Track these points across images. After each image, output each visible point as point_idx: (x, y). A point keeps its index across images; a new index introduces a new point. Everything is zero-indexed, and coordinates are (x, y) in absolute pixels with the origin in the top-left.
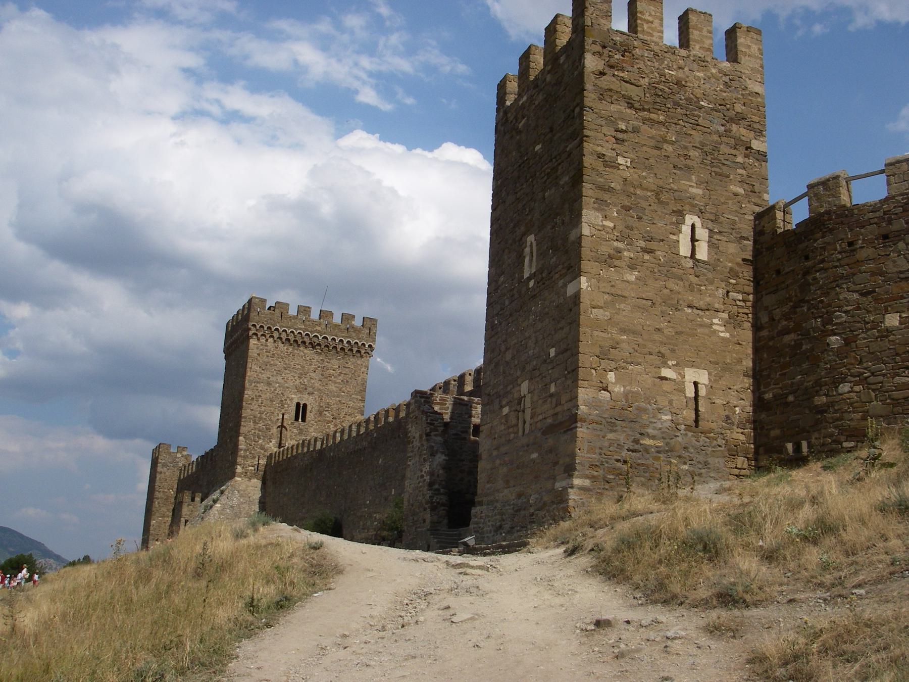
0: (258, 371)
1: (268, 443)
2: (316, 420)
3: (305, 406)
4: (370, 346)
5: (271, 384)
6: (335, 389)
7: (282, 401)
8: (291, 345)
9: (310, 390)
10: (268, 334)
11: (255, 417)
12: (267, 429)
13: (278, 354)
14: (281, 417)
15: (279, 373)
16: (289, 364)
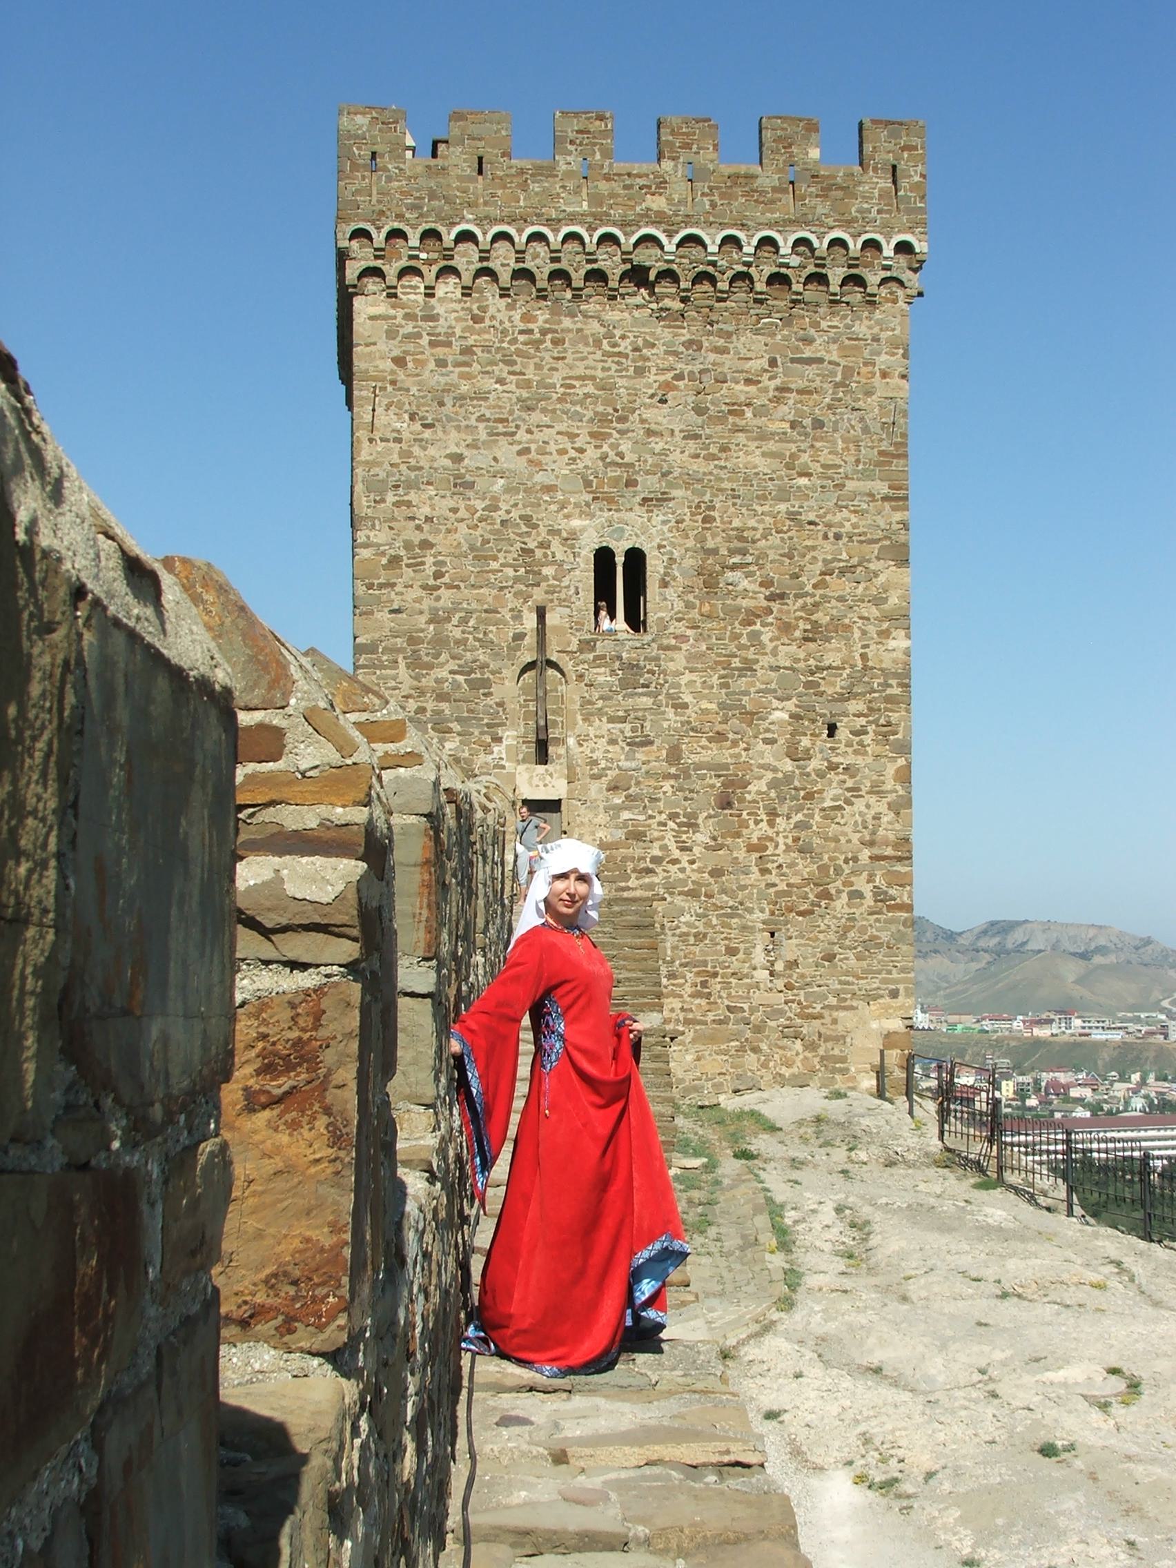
0: (406, 435)
1: (487, 749)
2: (694, 614)
3: (636, 558)
4: (904, 248)
5: (471, 485)
6: (764, 466)
7: (527, 552)
8: (542, 296)
9: (650, 484)
10: (429, 262)
11: (412, 641)
12: (474, 685)
13: (486, 348)
14: (530, 621)
15: (501, 428)
16: (541, 384)
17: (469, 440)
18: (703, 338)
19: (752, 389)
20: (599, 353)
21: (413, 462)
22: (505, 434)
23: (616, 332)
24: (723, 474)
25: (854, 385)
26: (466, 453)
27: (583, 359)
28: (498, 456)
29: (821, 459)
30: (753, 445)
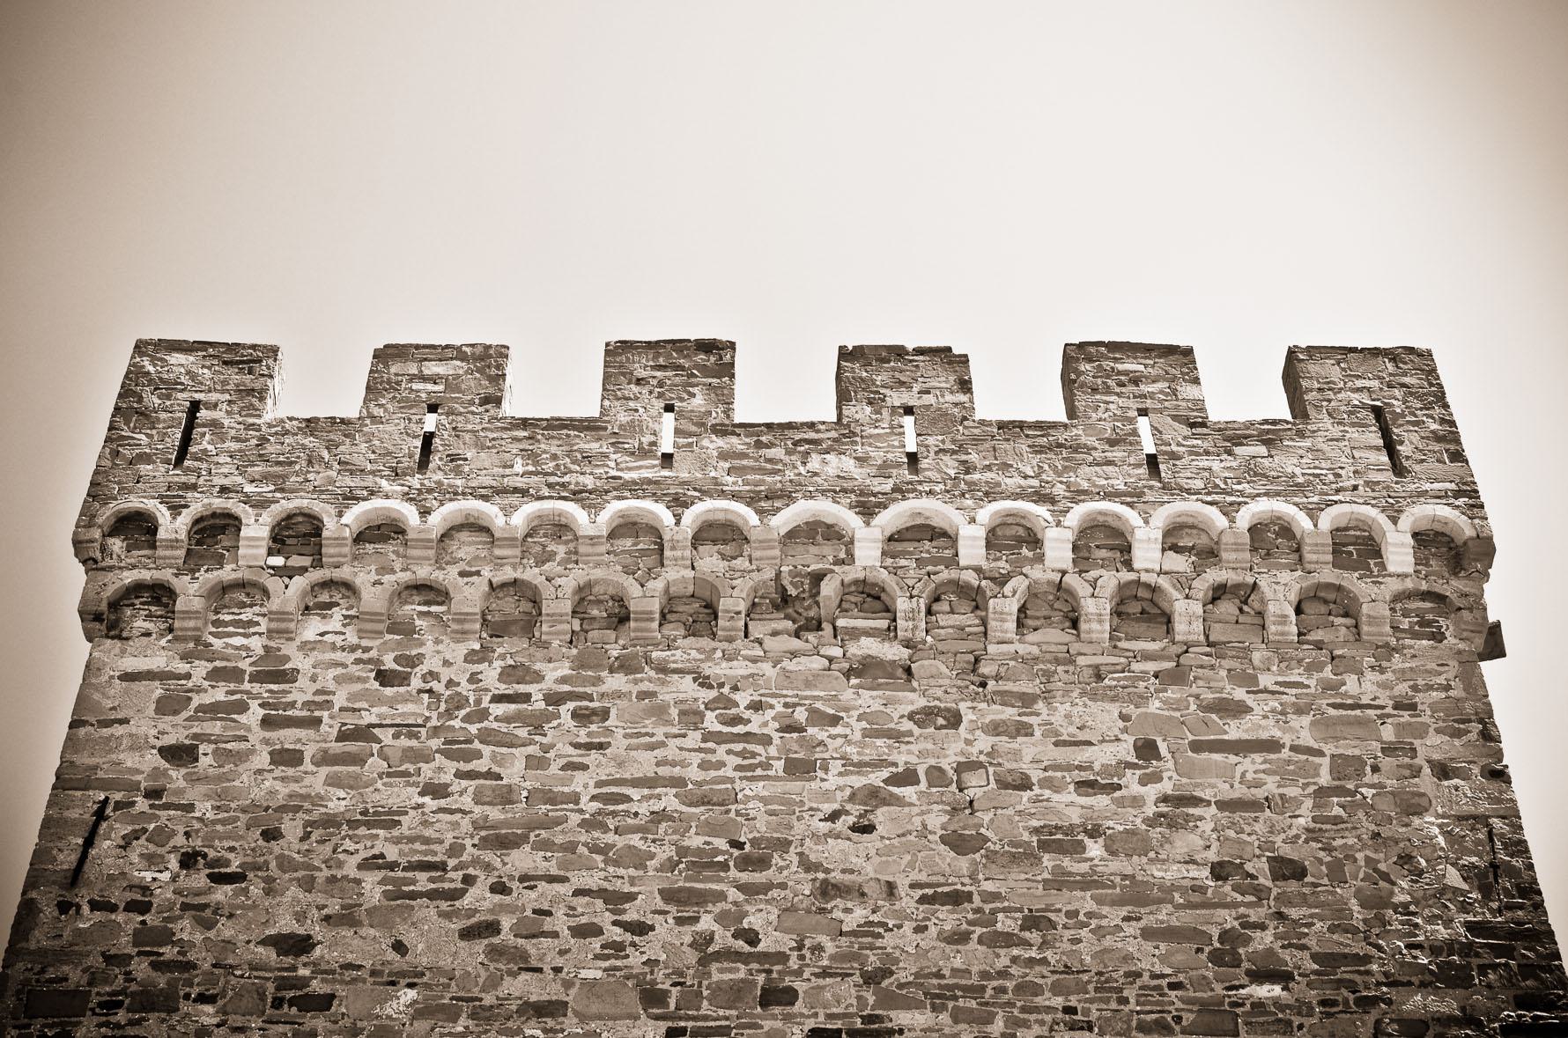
0: (163, 895)
15: (423, 881)
17: (334, 907)
18: (963, 707)
19: (1101, 801)
20: (694, 739)
21: (169, 952)
22: (433, 895)
23: (737, 697)
24: (1033, 975)
25: (1369, 792)
26: (318, 931)
27: (652, 747)
28: (409, 938)
29: (1312, 942)
30: (1114, 915)
